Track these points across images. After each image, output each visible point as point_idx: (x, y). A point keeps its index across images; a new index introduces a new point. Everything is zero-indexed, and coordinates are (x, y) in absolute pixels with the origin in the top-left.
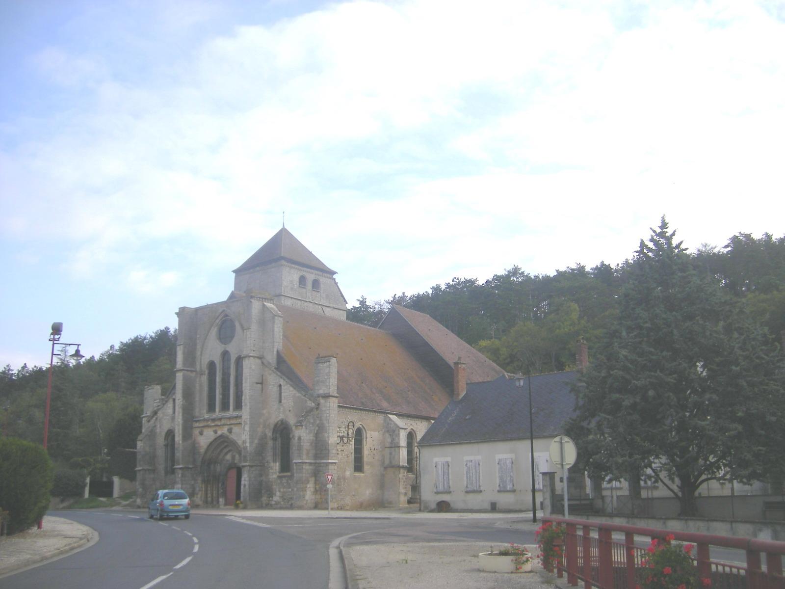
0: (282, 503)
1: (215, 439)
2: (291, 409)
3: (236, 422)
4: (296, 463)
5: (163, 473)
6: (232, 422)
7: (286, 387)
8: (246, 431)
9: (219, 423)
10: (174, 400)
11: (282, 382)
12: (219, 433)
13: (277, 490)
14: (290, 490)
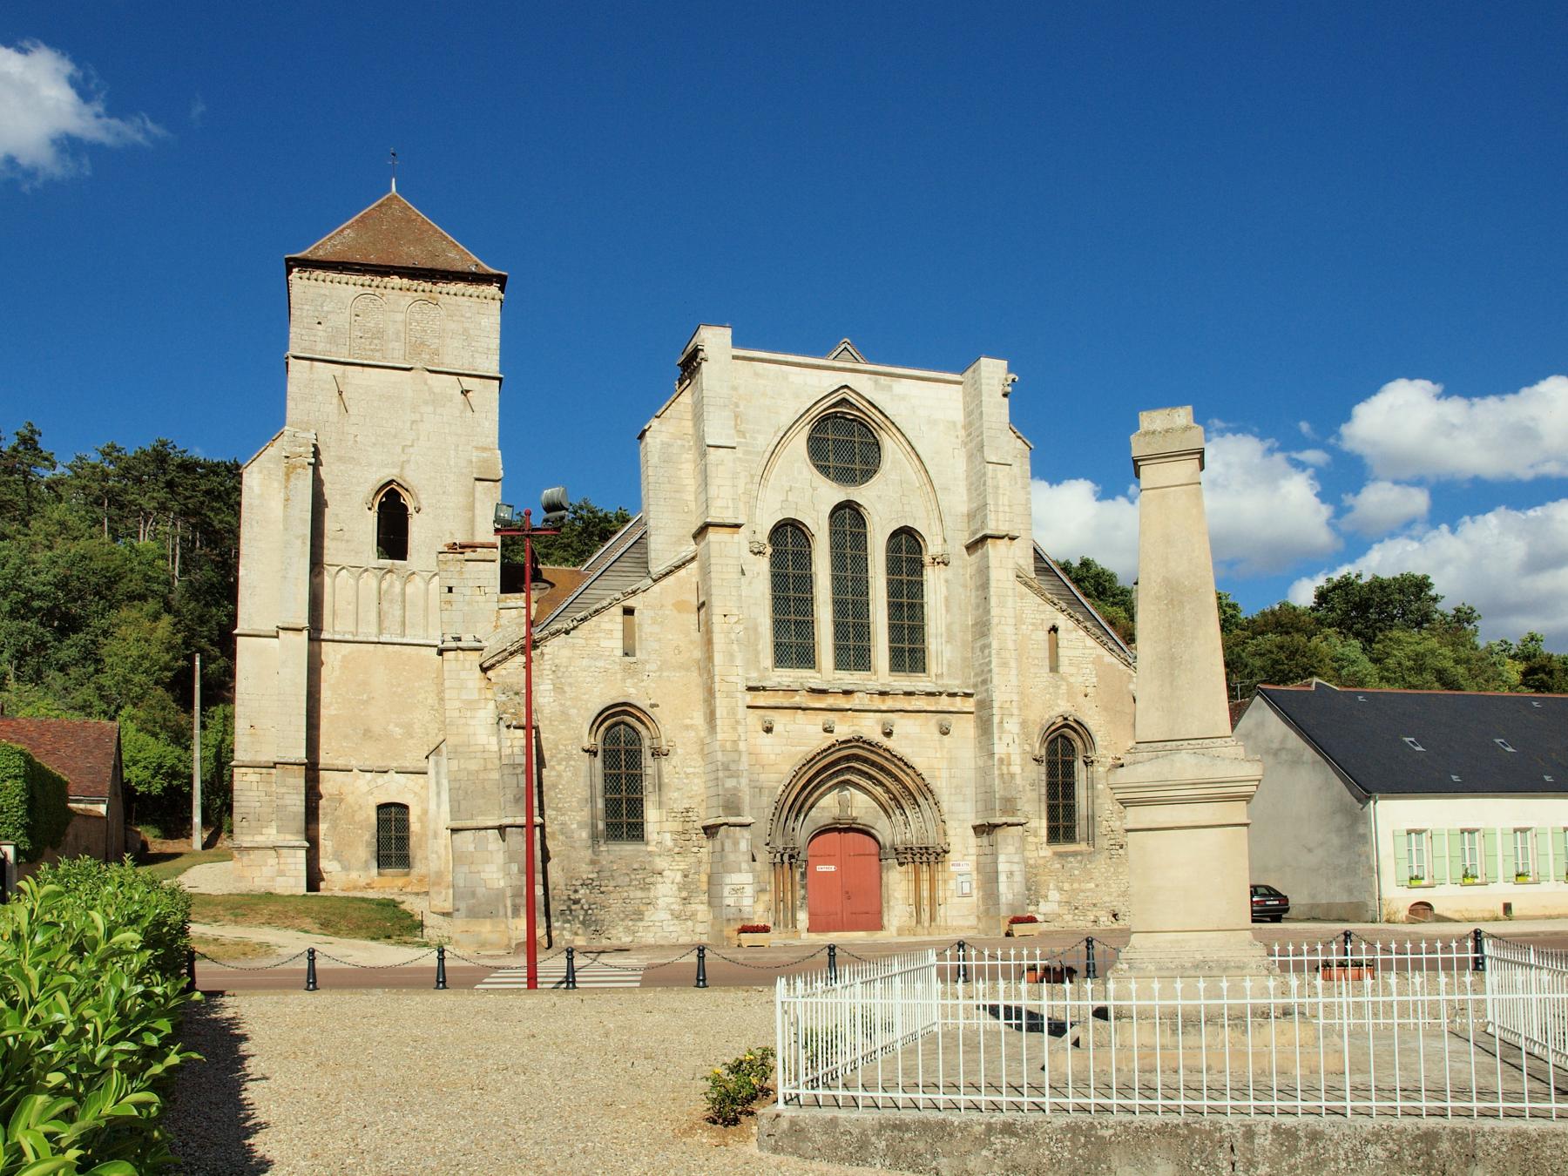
0: (1069, 917)
1: (829, 748)
3: (823, 706)
6: (889, 703)
7: (1074, 635)
8: (1010, 732)
9: (842, 702)
10: (628, 611)
11: (1062, 621)
12: (843, 730)
13: (1051, 886)
14: (1092, 885)
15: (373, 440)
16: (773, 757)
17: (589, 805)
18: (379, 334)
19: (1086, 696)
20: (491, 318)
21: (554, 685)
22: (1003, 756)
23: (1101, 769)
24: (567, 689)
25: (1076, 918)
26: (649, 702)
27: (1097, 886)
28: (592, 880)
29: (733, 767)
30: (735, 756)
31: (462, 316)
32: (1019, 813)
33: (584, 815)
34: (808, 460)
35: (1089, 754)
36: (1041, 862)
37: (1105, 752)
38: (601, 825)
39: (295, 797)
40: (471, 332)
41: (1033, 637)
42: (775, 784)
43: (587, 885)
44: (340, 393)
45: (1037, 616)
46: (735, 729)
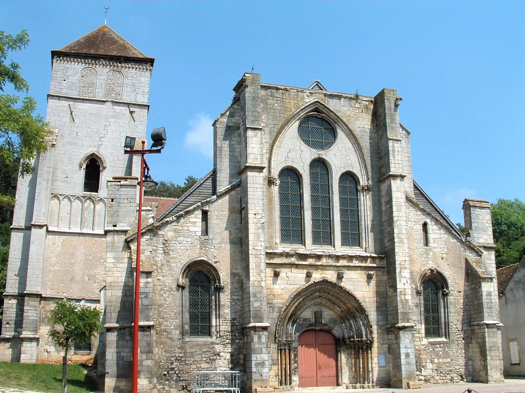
0: (437, 378)
2: (444, 256)
4: (487, 325)
5: (176, 334)
10: (205, 214)
11: (428, 221)
12: (317, 276)
15: (86, 134)
16: (280, 290)
17: (181, 316)
18: (92, 85)
19: (442, 259)
20: (147, 78)
21: (164, 250)
22: (402, 290)
23: (451, 297)
24: (171, 253)
25: (441, 378)
26: (214, 260)
27: (452, 360)
28: (181, 357)
29: (258, 295)
30: (260, 289)
31: (132, 77)
32: (411, 321)
33: (177, 322)
34: (299, 137)
35: (445, 290)
36: (422, 347)
37: (453, 288)
38: (187, 327)
39: (34, 312)
40: (136, 84)
41: (415, 228)
42: (281, 305)
43: (178, 360)
44: (71, 113)
45: (416, 217)
46: (259, 275)
